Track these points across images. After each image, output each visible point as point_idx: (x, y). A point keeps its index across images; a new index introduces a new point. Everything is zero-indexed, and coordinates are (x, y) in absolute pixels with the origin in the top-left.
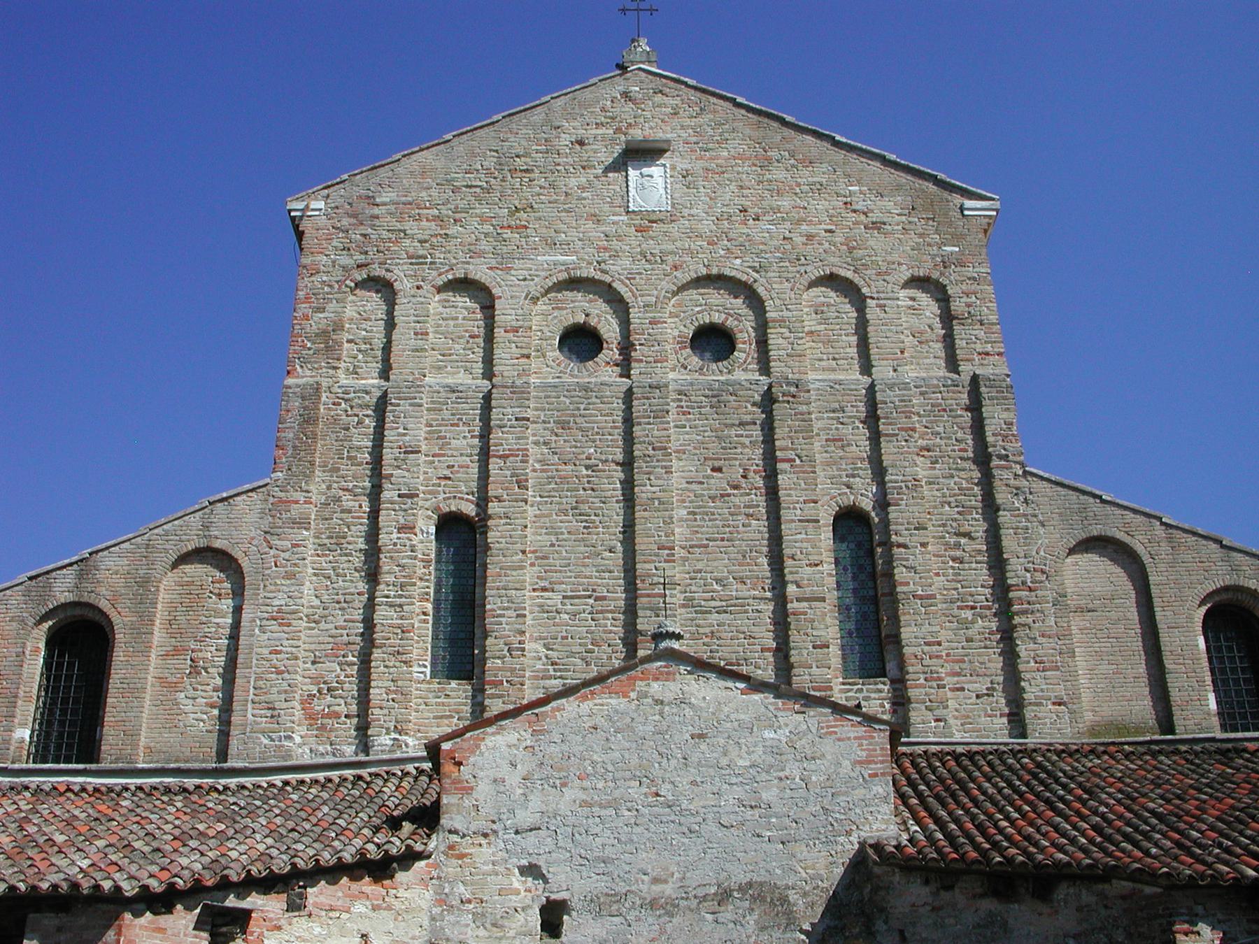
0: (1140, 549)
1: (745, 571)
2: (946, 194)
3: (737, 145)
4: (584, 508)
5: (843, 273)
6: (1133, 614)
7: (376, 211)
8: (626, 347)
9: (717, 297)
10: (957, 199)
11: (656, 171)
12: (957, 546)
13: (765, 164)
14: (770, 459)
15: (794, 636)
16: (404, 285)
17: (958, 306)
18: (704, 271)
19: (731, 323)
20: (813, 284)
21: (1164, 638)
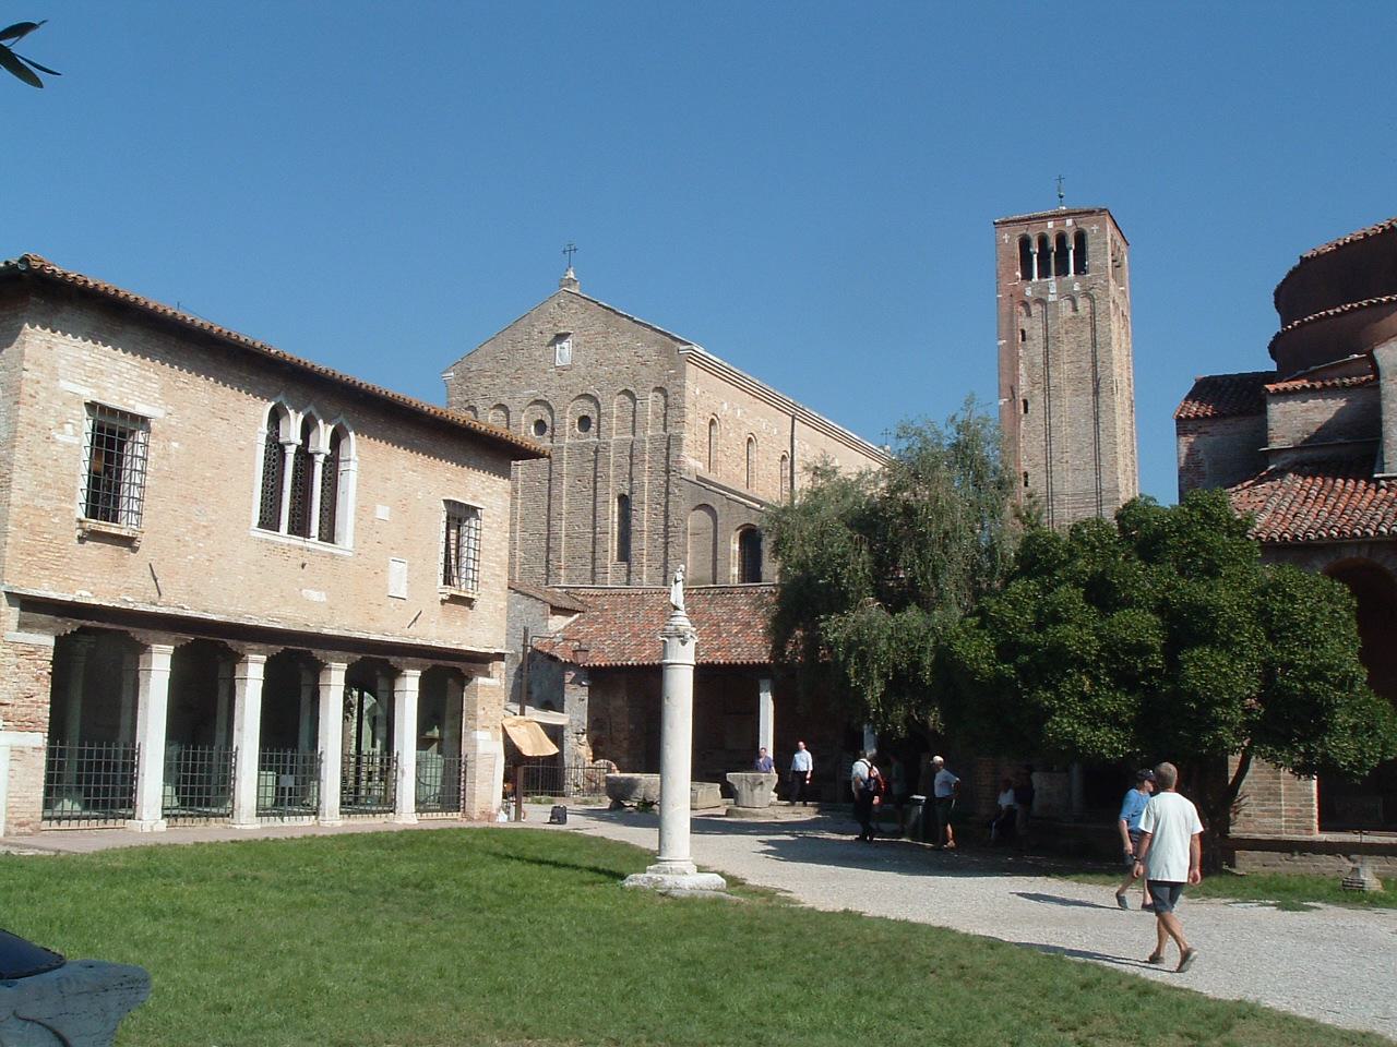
0: (717, 509)
1: (586, 522)
2: (674, 343)
3: (599, 327)
4: (537, 499)
5: (629, 388)
6: (712, 535)
7: (470, 375)
8: (553, 430)
9: (585, 403)
10: (678, 345)
11: (565, 344)
12: (656, 509)
13: (606, 335)
14: (596, 476)
15: (597, 547)
16: (480, 409)
17: (670, 400)
18: (580, 393)
19: (590, 415)
20: (619, 394)
21: (719, 546)
